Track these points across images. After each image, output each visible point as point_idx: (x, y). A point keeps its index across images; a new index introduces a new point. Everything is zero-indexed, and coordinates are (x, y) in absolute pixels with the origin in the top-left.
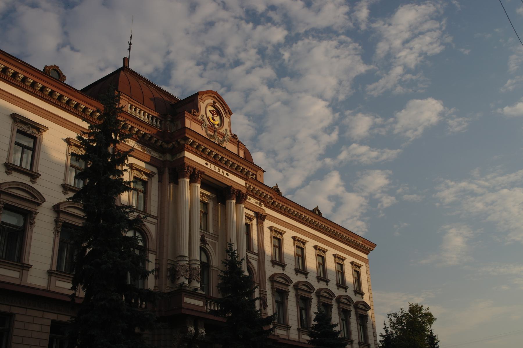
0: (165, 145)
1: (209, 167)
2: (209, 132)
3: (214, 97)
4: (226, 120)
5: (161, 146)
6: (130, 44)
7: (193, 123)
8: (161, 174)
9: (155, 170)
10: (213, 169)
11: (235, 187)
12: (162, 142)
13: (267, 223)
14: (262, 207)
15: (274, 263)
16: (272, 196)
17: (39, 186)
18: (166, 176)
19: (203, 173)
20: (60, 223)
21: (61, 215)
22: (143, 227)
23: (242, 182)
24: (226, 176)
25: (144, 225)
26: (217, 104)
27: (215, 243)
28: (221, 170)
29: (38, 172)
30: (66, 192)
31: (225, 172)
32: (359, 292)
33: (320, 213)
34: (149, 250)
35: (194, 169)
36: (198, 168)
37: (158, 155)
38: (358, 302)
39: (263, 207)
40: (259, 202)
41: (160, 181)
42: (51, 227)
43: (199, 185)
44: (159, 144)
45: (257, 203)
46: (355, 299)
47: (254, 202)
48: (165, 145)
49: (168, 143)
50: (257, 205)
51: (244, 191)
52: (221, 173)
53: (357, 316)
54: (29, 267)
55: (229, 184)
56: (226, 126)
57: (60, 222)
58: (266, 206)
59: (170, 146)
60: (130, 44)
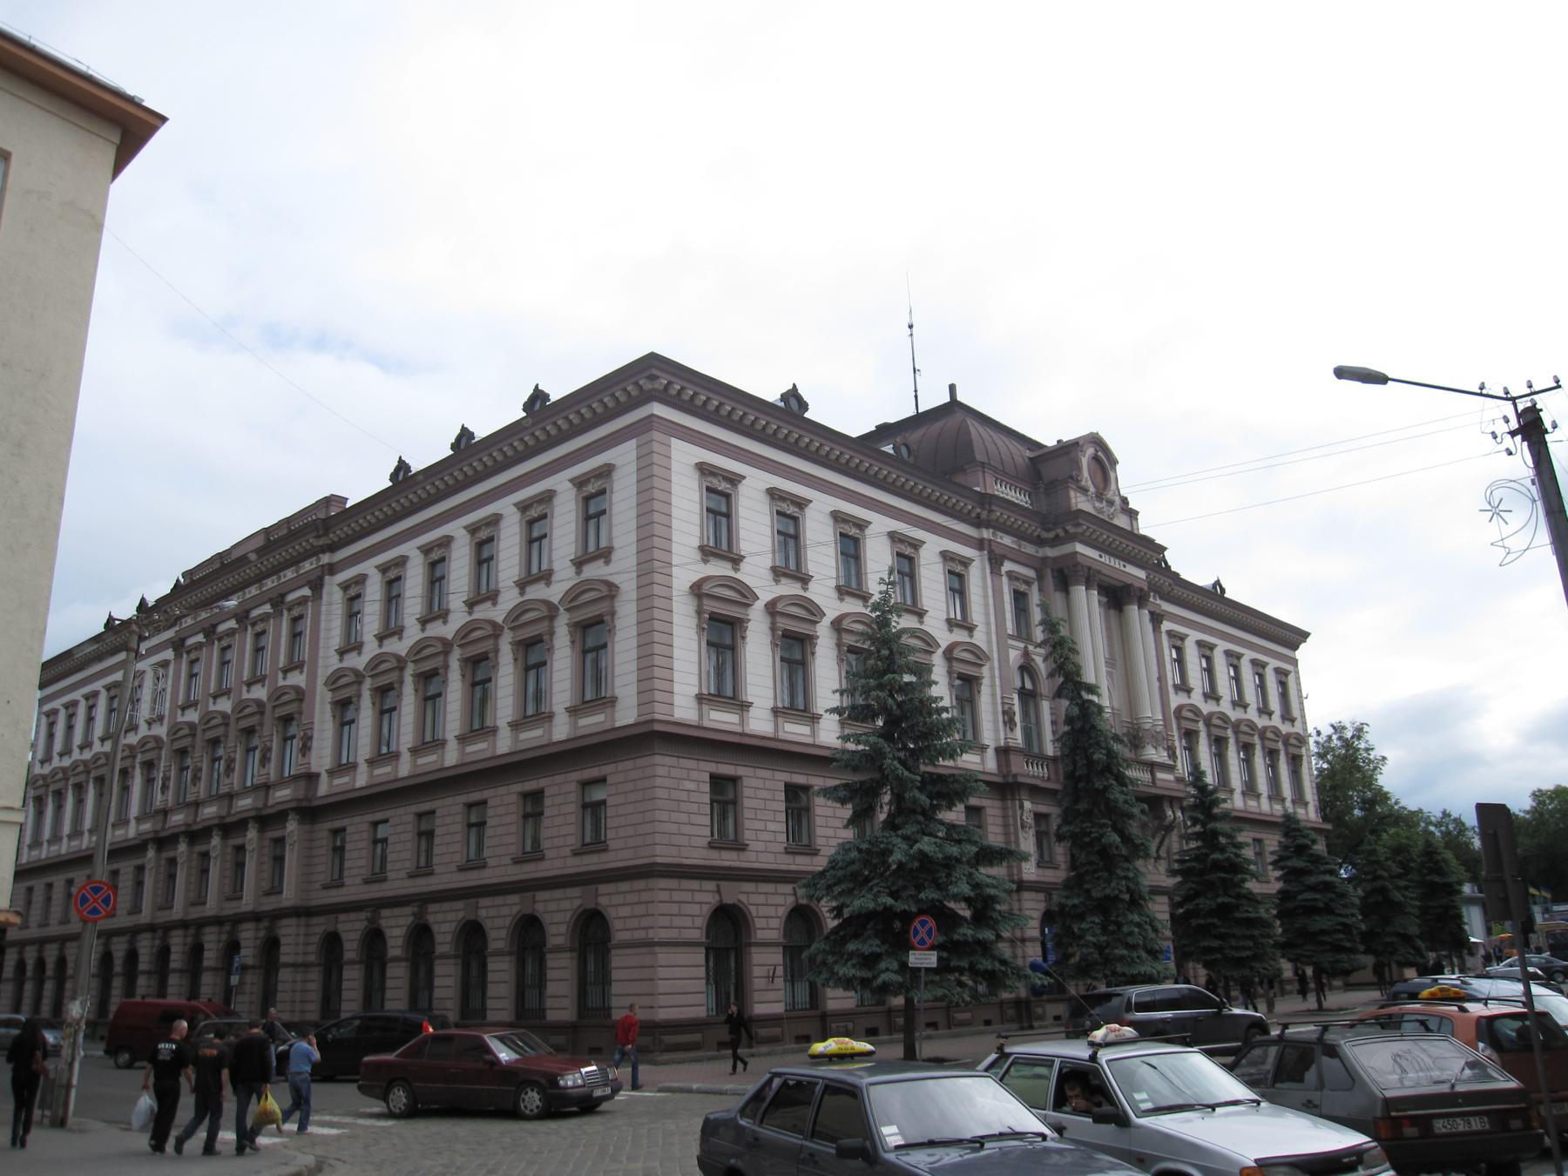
0: (1045, 535)
1: (1103, 560)
2: (1097, 504)
3: (1095, 443)
4: (1112, 475)
5: (1039, 536)
6: (911, 327)
7: (1078, 494)
8: (1040, 577)
9: (1030, 573)
10: (1112, 564)
11: (1137, 584)
13: (1166, 626)
15: (1177, 688)
18: (1049, 581)
19: (1099, 572)
22: (1032, 664)
23: (1142, 574)
24: (1122, 568)
25: (1033, 660)
26: (1100, 453)
28: (1117, 561)
31: (1122, 563)
32: (1287, 717)
33: (1223, 591)
34: (1041, 695)
35: (1089, 568)
36: (1096, 567)
38: (1265, 729)
39: (1158, 602)
41: (1041, 590)
43: (1096, 592)
44: (1036, 534)
46: (1285, 728)
49: (1048, 530)
51: (1146, 588)
52: (1117, 566)
53: (1264, 751)
55: (1129, 582)
56: (1113, 487)
58: (1161, 598)
59: (1051, 535)
60: (911, 327)
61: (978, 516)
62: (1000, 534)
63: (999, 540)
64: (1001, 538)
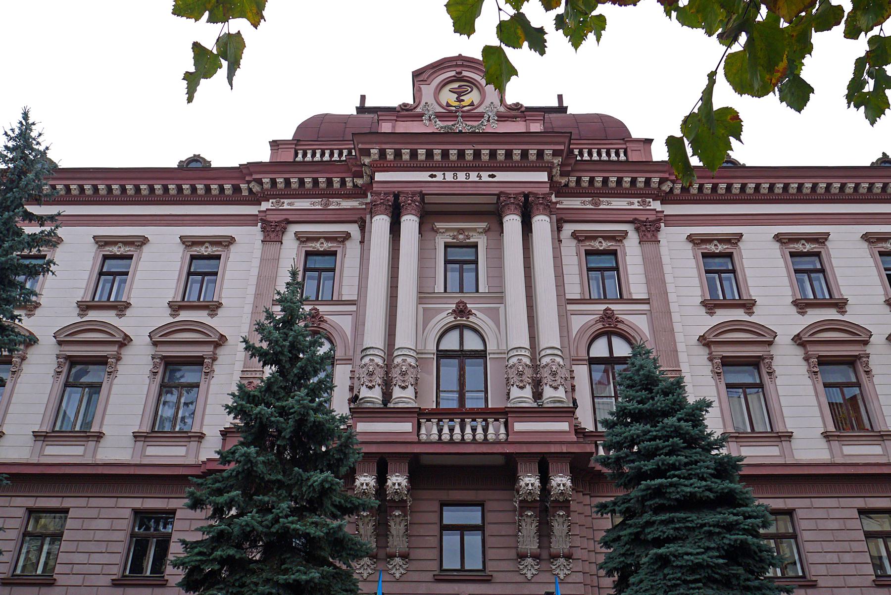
5: (355, 186)
12: (351, 179)
14: (650, 206)
16: (662, 175)
17: (758, 317)
20: (813, 360)
21: (809, 348)
27: (498, 309)
29: (631, 296)
30: (751, 311)
37: (308, 204)
40: (636, 200)
42: (803, 368)
45: (633, 204)
47: (625, 203)
48: (359, 182)
50: (636, 206)
54: (789, 436)
57: (811, 358)
61: (250, 190)
62: (286, 201)
63: (289, 207)
64: (289, 204)
